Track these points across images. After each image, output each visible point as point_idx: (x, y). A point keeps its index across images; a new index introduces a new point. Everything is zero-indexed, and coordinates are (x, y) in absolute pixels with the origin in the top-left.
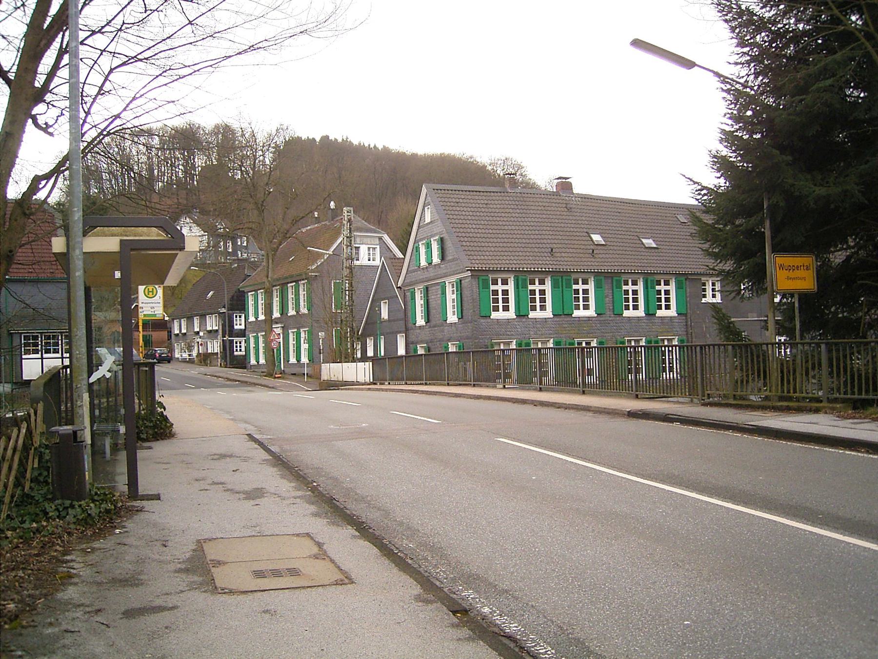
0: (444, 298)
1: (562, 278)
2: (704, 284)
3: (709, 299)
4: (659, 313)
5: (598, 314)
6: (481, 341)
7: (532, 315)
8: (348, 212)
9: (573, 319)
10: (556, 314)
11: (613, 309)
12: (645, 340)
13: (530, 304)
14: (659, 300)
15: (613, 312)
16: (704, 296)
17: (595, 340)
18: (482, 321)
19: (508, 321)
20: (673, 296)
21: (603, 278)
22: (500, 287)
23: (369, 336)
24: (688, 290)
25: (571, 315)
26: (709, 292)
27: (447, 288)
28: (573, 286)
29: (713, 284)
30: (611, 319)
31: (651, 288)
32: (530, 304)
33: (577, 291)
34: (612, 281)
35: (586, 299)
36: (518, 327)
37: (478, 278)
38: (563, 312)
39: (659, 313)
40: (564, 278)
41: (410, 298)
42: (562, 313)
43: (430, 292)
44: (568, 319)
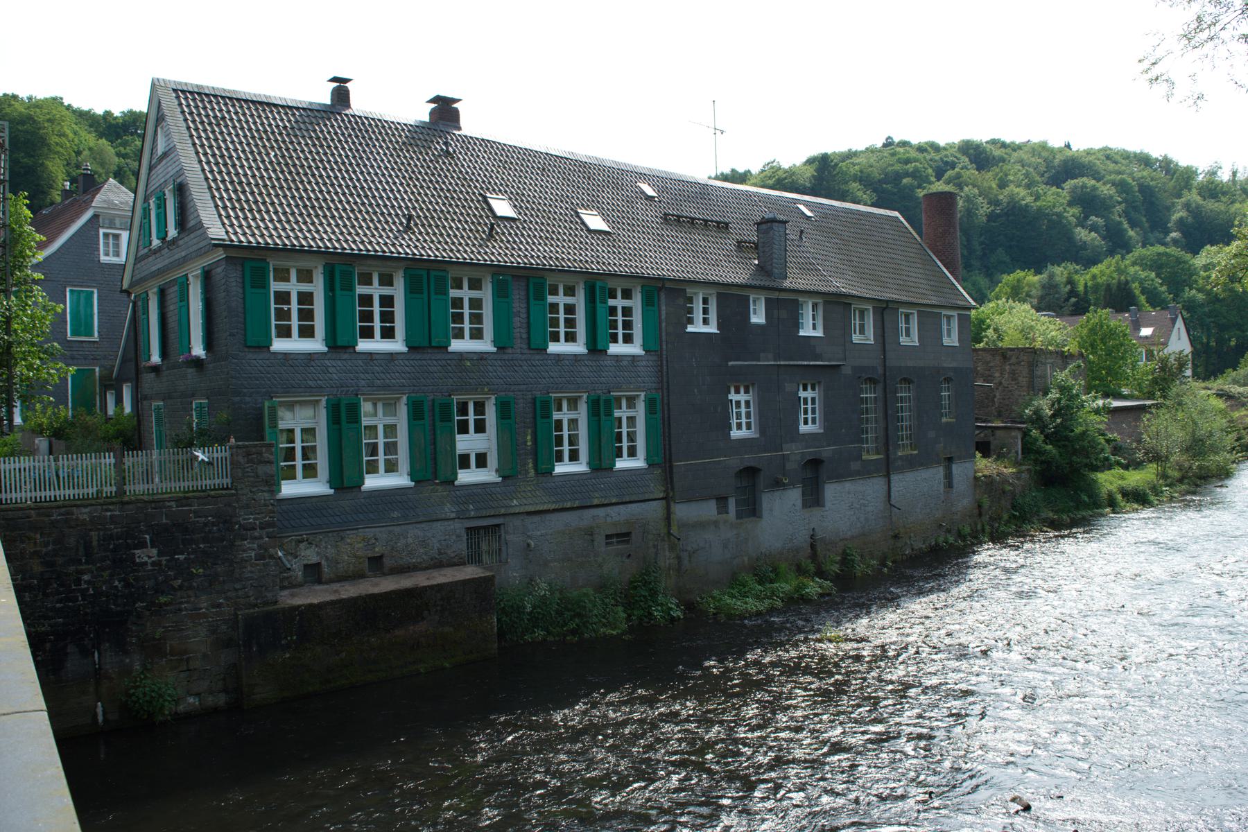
0: (184, 310)
1: (428, 274)
2: (691, 300)
3: (697, 328)
6: (247, 399)
7: (364, 345)
9: (450, 357)
11: (529, 338)
13: (359, 324)
14: (613, 325)
15: (529, 344)
16: (691, 321)
17: (493, 397)
18: (250, 356)
19: (310, 357)
21: (510, 278)
22: (294, 287)
23: (126, 381)
24: (663, 308)
25: (446, 348)
26: (698, 315)
27: (191, 288)
28: (451, 291)
29: (705, 301)
32: (359, 324)
33: (458, 303)
34: (528, 286)
35: (476, 318)
37: (243, 265)
39: (616, 349)
40: (433, 273)
42: (426, 344)
43: (168, 297)
44: (439, 357)
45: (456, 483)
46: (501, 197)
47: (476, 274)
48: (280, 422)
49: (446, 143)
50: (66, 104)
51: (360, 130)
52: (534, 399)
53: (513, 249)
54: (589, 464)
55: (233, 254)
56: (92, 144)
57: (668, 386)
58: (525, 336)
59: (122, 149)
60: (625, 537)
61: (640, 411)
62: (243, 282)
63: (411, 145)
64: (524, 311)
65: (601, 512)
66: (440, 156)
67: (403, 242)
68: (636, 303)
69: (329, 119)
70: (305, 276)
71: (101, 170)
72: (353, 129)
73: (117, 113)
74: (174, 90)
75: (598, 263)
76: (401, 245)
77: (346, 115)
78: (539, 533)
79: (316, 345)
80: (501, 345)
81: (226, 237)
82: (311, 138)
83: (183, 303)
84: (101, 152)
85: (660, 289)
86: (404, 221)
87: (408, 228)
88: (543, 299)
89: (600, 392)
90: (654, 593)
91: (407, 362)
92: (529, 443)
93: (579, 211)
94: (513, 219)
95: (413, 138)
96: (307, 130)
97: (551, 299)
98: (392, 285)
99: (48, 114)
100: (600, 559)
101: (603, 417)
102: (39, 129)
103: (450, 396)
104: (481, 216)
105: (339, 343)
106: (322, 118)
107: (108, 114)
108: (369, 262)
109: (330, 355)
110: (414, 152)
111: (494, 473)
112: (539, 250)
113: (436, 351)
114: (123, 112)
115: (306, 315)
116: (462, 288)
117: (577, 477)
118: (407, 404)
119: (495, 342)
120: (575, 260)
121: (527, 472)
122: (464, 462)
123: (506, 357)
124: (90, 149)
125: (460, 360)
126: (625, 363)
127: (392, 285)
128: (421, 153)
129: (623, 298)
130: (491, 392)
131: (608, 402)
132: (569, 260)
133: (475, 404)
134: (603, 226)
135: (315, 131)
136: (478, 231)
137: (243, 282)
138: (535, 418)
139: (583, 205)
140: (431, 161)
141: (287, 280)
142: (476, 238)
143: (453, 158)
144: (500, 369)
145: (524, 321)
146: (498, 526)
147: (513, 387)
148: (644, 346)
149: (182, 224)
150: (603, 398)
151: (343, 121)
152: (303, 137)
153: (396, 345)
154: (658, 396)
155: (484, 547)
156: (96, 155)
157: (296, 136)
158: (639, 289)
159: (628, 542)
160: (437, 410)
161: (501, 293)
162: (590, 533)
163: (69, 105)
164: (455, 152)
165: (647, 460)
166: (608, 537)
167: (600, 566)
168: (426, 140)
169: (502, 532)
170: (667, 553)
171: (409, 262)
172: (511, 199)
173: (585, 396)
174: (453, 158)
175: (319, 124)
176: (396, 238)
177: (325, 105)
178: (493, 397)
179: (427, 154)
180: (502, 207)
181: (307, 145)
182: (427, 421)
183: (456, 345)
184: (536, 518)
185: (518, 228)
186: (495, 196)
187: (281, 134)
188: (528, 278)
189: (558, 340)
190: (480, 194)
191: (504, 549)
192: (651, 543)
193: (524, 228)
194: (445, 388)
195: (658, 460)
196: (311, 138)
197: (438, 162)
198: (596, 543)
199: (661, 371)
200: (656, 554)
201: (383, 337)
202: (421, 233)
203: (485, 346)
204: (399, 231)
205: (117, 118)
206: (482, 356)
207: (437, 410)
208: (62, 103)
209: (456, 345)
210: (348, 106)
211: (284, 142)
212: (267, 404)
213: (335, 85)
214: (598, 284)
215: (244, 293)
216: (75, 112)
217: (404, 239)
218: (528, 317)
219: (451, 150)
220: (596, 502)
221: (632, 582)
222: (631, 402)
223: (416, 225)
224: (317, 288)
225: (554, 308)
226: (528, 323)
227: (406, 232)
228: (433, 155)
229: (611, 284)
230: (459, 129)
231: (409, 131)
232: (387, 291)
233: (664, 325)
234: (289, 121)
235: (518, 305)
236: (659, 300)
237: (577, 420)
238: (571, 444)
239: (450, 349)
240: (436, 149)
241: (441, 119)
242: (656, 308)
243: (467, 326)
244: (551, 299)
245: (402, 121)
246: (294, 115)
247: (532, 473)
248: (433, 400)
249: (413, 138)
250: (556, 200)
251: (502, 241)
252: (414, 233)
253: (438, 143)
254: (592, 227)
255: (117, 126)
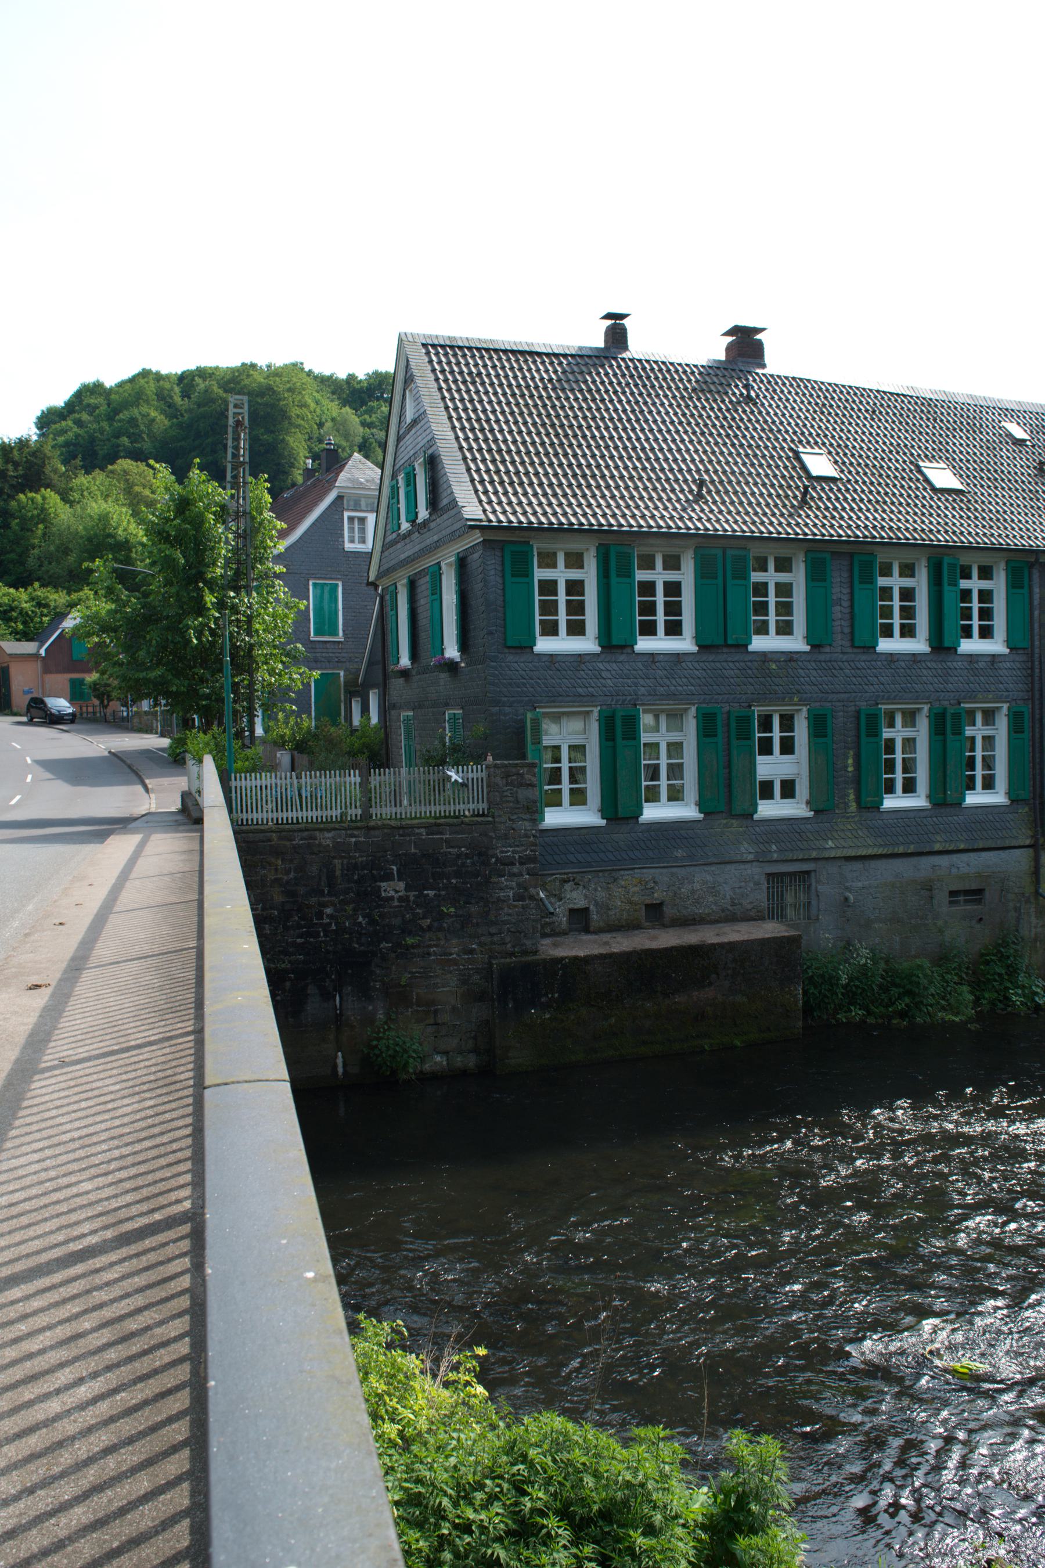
0: (436, 604)
1: (724, 553)
4: (967, 646)
5: (813, 646)
6: (507, 709)
7: (644, 644)
8: (236, 406)
9: (750, 657)
10: (708, 643)
11: (852, 633)
12: (930, 710)
13: (638, 618)
14: (967, 614)
15: (852, 640)
17: (805, 709)
18: (510, 658)
19: (580, 658)
20: (999, 606)
21: (828, 556)
22: (561, 574)
23: (373, 686)
24: (1036, 590)
25: (746, 646)
27: (444, 578)
28: (753, 574)
30: (845, 658)
31: (949, 585)
32: (638, 618)
33: (761, 589)
34: (851, 565)
35: (785, 608)
36: (604, 674)
37: (502, 550)
38: (726, 640)
39: (967, 646)
41: (389, 608)
42: (721, 642)
43: (419, 590)
44: (737, 657)
45: (756, 817)
46: (817, 450)
47: (784, 552)
48: (544, 737)
49: (747, 387)
50: (307, 370)
51: (640, 377)
52: (858, 712)
53: (833, 517)
54: (929, 797)
55: (492, 536)
56: (335, 414)
57: (1041, 695)
58: (847, 630)
59: (367, 417)
60: (975, 894)
61: (1001, 729)
62: (503, 570)
63: (702, 391)
64: (846, 597)
65: (943, 861)
66: (739, 403)
67: (693, 514)
68: (998, 585)
69: (603, 366)
70: (575, 561)
71: (344, 444)
72: (632, 376)
73: (361, 376)
74: (423, 345)
75: (946, 532)
76: (691, 519)
77: (623, 359)
78: (860, 884)
79: (587, 644)
80: (817, 643)
81: (483, 517)
82: (581, 391)
83: (435, 597)
84: (345, 422)
85: (1031, 566)
86: (694, 487)
87: (699, 496)
88: (872, 581)
89: (946, 703)
90: (1012, 971)
91: (696, 665)
92: (850, 769)
93: (921, 464)
94: (833, 480)
95: (706, 382)
96: (577, 381)
97: (882, 582)
98: (679, 569)
99: (288, 382)
100: (940, 923)
101: (950, 736)
102: (279, 400)
103: (750, 706)
104: (792, 477)
105: (615, 642)
106: (594, 365)
107: (351, 377)
108: (652, 541)
109: (603, 656)
110: (707, 400)
111: (804, 806)
112: (867, 518)
113: (733, 650)
114: (368, 374)
115: (576, 608)
116: (766, 570)
117: (912, 815)
118: (696, 717)
119: (808, 638)
120: (915, 530)
121: (847, 805)
122: (766, 790)
123: (822, 657)
124: (333, 420)
125: (764, 662)
126: (982, 665)
127: (679, 569)
128: (715, 401)
129: (980, 578)
130: (802, 702)
131: (957, 717)
132: (907, 529)
133: (782, 717)
134: (954, 483)
135: (585, 382)
136: (787, 496)
137: (503, 570)
138: (858, 737)
139: (926, 456)
140: (728, 410)
141: (554, 566)
142: (785, 506)
143: (755, 404)
144: (814, 673)
145: (847, 610)
146: (808, 873)
147: (831, 696)
148: (1008, 642)
149: (433, 504)
150: (951, 710)
151: (619, 367)
152: (572, 390)
153: (685, 644)
154: (1026, 709)
155: (789, 898)
156: (340, 426)
157: (563, 390)
158: (1003, 565)
159: (979, 901)
160: (733, 724)
161: (816, 575)
162: (928, 887)
163: (310, 371)
164: (758, 396)
165: (1009, 794)
166: (952, 893)
167: (941, 931)
168: (721, 384)
169: (813, 881)
170: (1033, 920)
171: (700, 540)
172: (830, 453)
173: (926, 708)
174: (755, 404)
175: (590, 374)
176: (684, 509)
177: (597, 349)
178: (805, 709)
179: (723, 401)
180: (819, 464)
181: (576, 399)
182: (720, 738)
183: (758, 643)
184: (858, 865)
185: (839, 490)
186: (809, 450)
187: (545, 388)
188: (851, 555)
189: (891, 635)
190: (791, 449)
191: (814, 903)
192: (1011, 905)
193: (847, 490)
194: (744, 697)
195: (1025, 794)
196: (581, 391)
197: (736, 411)
198: (935, 902)
199: (1032, 676)
200: (1018, 919)
201: (667, 634)
202: (715, 502)
203: (796, 643)
204: (687, 501)
205: (361, 381)
206: (790, 657)
207: (733, 724)
208: (303, 369)
209: (758, 643)
210: (625, 347)
211: (549, 398)
212: (529, 715)
213: (609, 322)
214: (947, 560)
215: (504, 583)
216: (316, 378)
217: (694, 510)
218: (852, 606)
219: (753, 394)
220: (937, 847)
221: (982, 955)
222: (989, 717)
223: (709, 492)
224: (589, 575)
225: (886, 593)
226: (852, 614)
227: (696, 502)
228: (731, 402)
229: (964, 559)
230: (764, 366)
231: (700, 373)
232: (672, 576)
233: (1036, 613)
234: (555, 372)
235: (838, 589)
236: (1030, 579)
237: (914, 740)
238: (905, 770)
239: (751, 648)
240: (734, 394)
241: (741, 355)
242: (1025, 591)
243: (772, 618)
244: (882, 582)
245: (692, 361)
246: (560, 364)
247: (853, 806)
248: (729, 712)
249: (706, 382)
250: (891, 452)
251: (818, 508)
252: (706, 503)
253: (737, 386)
254: (938, 484)
255: (361, 391)
